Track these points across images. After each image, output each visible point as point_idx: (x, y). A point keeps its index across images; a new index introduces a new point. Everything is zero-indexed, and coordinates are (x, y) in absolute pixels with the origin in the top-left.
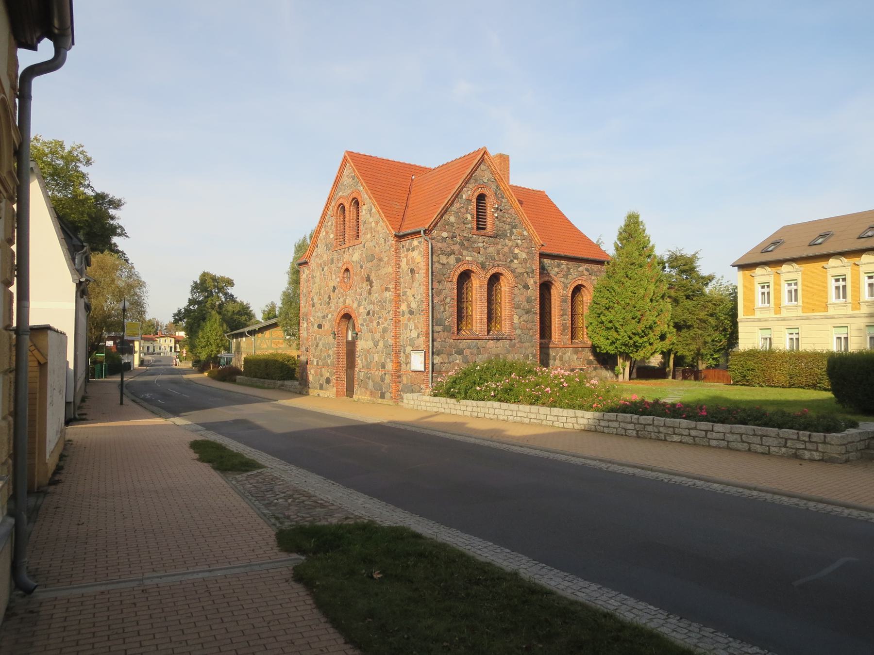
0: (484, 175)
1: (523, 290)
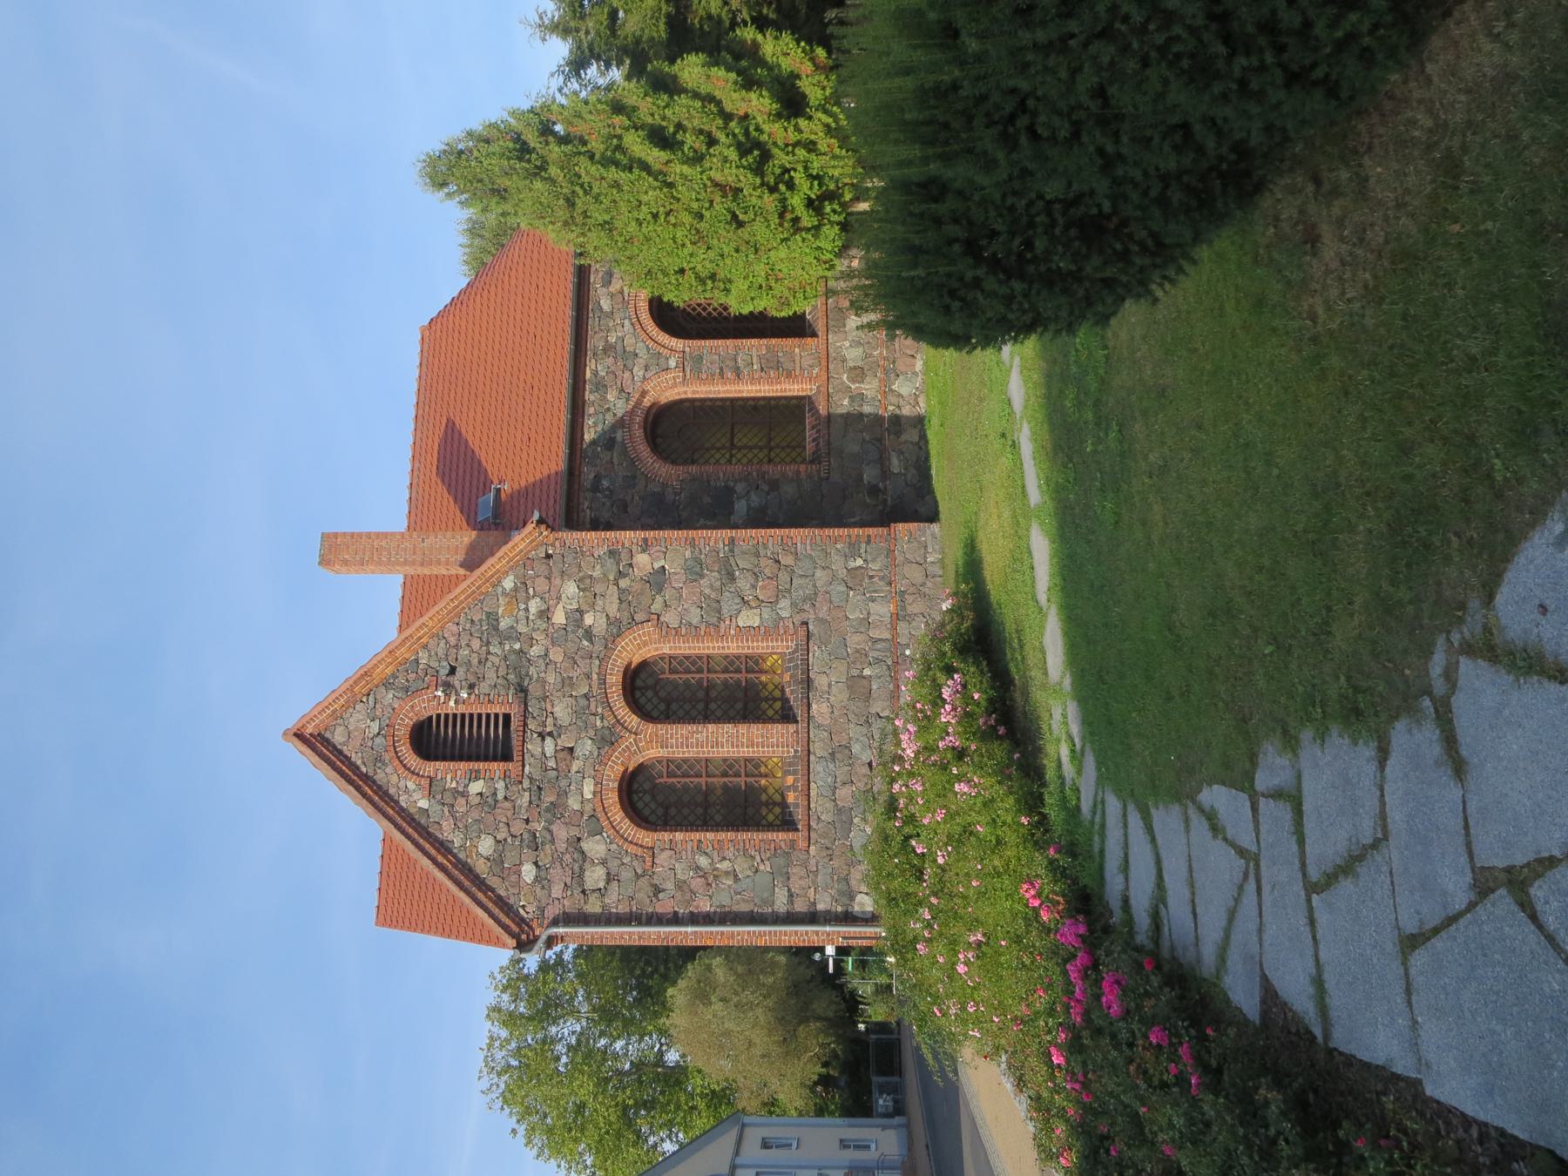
0: (357, 732)
1: (668, 593)
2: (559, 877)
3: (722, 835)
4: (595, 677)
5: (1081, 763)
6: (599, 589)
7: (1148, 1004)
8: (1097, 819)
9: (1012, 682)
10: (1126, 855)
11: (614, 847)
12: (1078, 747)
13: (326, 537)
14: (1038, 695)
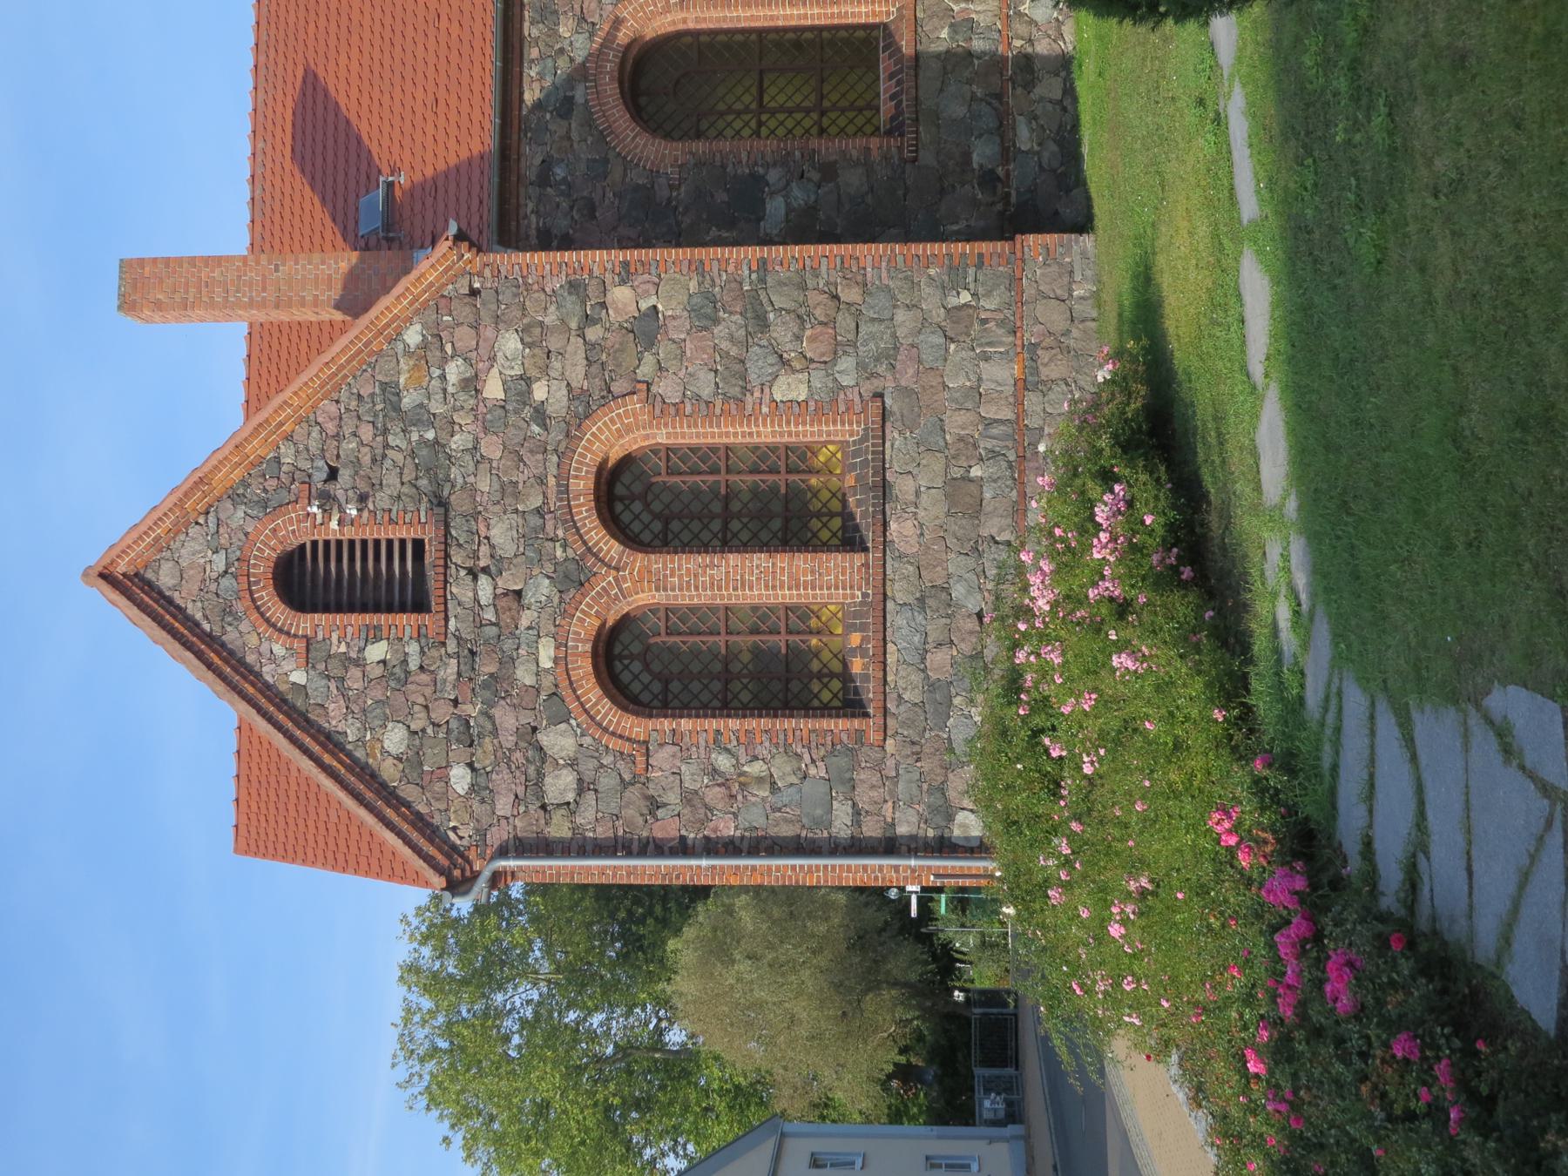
0: (192, 569)
1: (664, 349)
2: (505, 786)
3: (752, 723)
4: (552, 481)
5: (1308, 631)
6: (554, 343)
7: (1393, 1000)
8: (1330, 718)
9: (1204, 496)
10: (1372, 776)
11: (587, 741)
12: (1305, 607)
13: (126, 266)
14: (1246, 523)
